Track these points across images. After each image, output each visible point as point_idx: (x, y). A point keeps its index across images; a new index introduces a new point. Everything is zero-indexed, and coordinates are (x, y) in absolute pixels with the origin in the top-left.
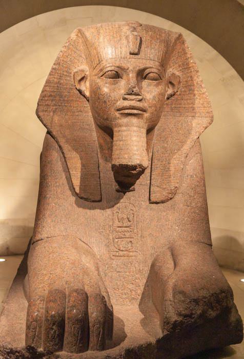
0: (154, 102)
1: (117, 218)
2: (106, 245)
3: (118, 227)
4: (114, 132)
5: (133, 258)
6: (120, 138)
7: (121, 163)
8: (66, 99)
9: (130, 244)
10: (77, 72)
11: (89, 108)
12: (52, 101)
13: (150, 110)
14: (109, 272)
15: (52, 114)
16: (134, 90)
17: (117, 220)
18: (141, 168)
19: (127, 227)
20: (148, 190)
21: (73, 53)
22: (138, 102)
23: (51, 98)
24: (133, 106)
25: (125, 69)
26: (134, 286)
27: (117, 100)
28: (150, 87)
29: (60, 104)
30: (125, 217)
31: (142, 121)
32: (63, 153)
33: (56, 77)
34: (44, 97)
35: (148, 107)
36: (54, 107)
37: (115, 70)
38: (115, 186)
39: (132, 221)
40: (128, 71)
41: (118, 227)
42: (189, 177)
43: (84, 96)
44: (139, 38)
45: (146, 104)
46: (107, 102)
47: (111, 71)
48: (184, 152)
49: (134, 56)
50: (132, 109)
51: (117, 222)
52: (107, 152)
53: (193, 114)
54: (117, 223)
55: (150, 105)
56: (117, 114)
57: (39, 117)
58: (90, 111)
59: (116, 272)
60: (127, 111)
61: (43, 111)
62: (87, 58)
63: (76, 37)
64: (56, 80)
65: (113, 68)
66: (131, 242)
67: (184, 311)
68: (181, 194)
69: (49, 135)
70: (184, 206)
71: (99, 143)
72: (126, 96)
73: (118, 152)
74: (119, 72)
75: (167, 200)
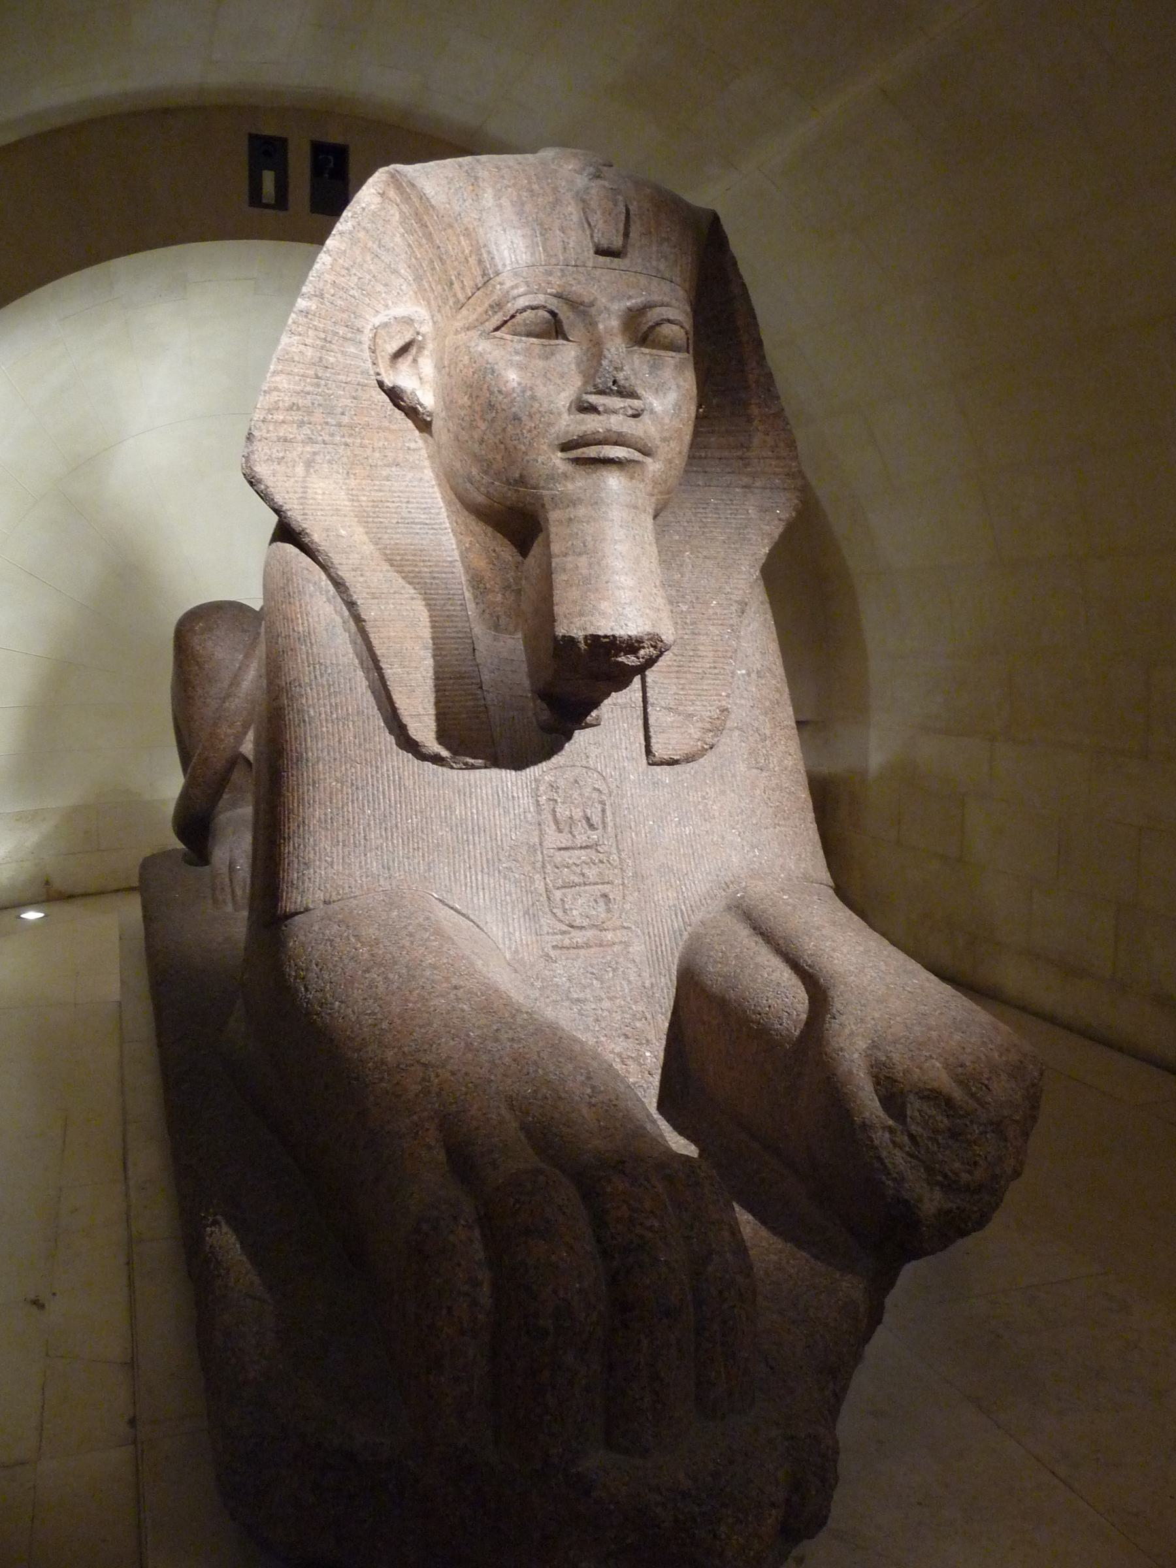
0: (676, 424)
1: (550, 818)
2: (526, 913)
3: (560, 849)
4: (551, 522)
5: (616, 948)
6: (578, 543)
7: (591, 631)
8: (346, 420)
9: (601, 902)
10: (385, 325)
11: (424, 453)
12: (301, 424)
13: (664, 451)
14: (548, 1006)
15: (300, 470)
16: (620, 376)
17: (552, 824)
18: (655, 647)
19: (586, 847)
20: (641, 722)
21: (368, 258)
22: (632, 421)
23: (297, 416)
24: (620, 434)
25: (582, 303)
26: (630, 1044)
27: (560, 414)
28: (659, 373)
29: (327, 438)
30: (578, 814)
31: (641, 486)
32: (351, 605)
33: (308, 341)
34: (269, 411)
35: (658, 442)
36: (308, 449)
37: (550, 307)
38: (536, 711)
39: (601, 827)
40: (593, 311)
41: (560, 849)
42: (754, 676)
43: (412, 412)
44: (620, 198)
45: (652, 430)
46: (525, 418)
47: (533, 308)
48: (734, 597)
49: (608, 259)
50: (616, 444)
51: (557, 833)
52: (499, 598)
53: (746, 480)
54: (553, 838)
55: (667, 434)
56: (558, 460)
57: (253, 481)
58: (427, 463)
59: (567, 1004)
60: (592, 452)
61: (270, 459)
62: (418, 279)
63: (378, 199)
64: (309, 352)
65: (540, 299)
66: (605, 896)
67: (970, 1172)
68: (737, 733)
69: (290, 548)
70: (749, 768)
71: (467, 568)
72: (593, 399)
73: (575, 593)
74: (561, 316)
75: (702, 752)
